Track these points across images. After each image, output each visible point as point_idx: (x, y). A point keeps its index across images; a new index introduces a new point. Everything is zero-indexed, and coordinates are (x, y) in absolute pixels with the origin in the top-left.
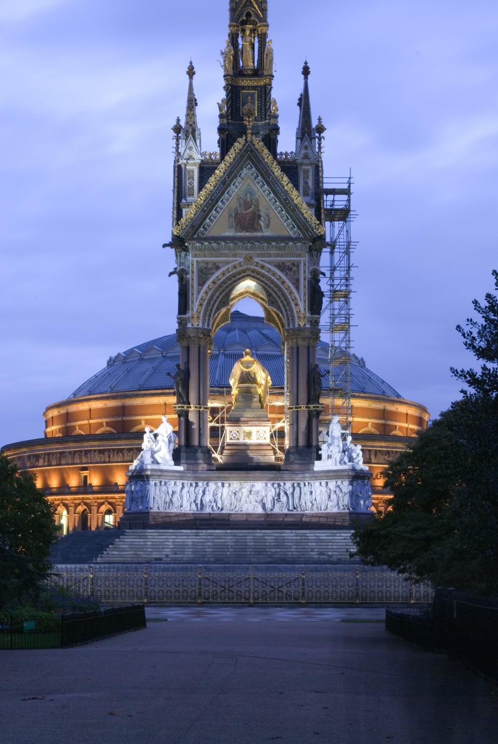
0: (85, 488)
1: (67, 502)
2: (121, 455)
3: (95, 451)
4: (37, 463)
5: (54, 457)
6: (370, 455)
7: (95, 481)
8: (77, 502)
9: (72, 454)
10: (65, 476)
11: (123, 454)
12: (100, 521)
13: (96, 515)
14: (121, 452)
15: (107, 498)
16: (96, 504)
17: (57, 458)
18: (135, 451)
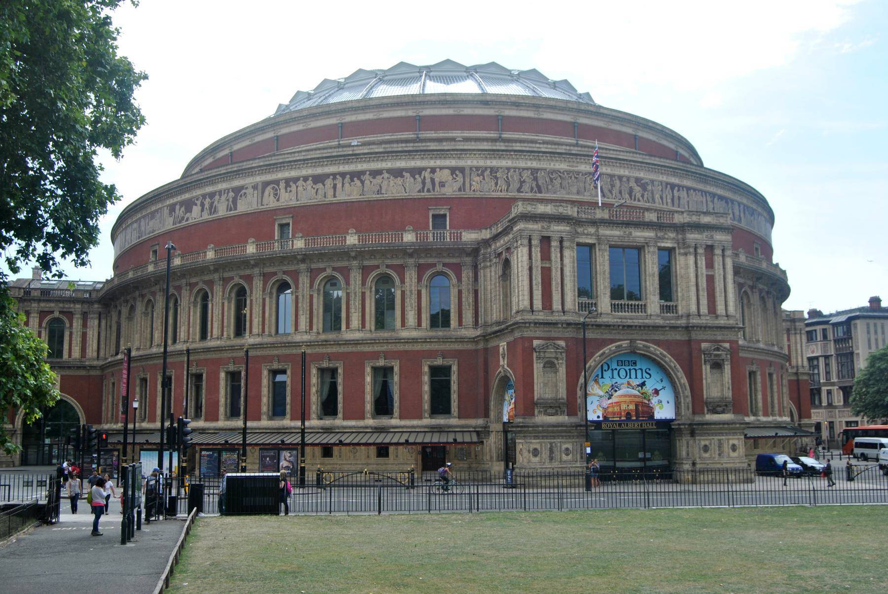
2: (357, 182)
3: (306, 179)
4: (188, 214)
5: (223, 198)
9: (260, 187)
11: (362, 182)
14: (359, 179)
17: (228, 200)
18: (386, 175)
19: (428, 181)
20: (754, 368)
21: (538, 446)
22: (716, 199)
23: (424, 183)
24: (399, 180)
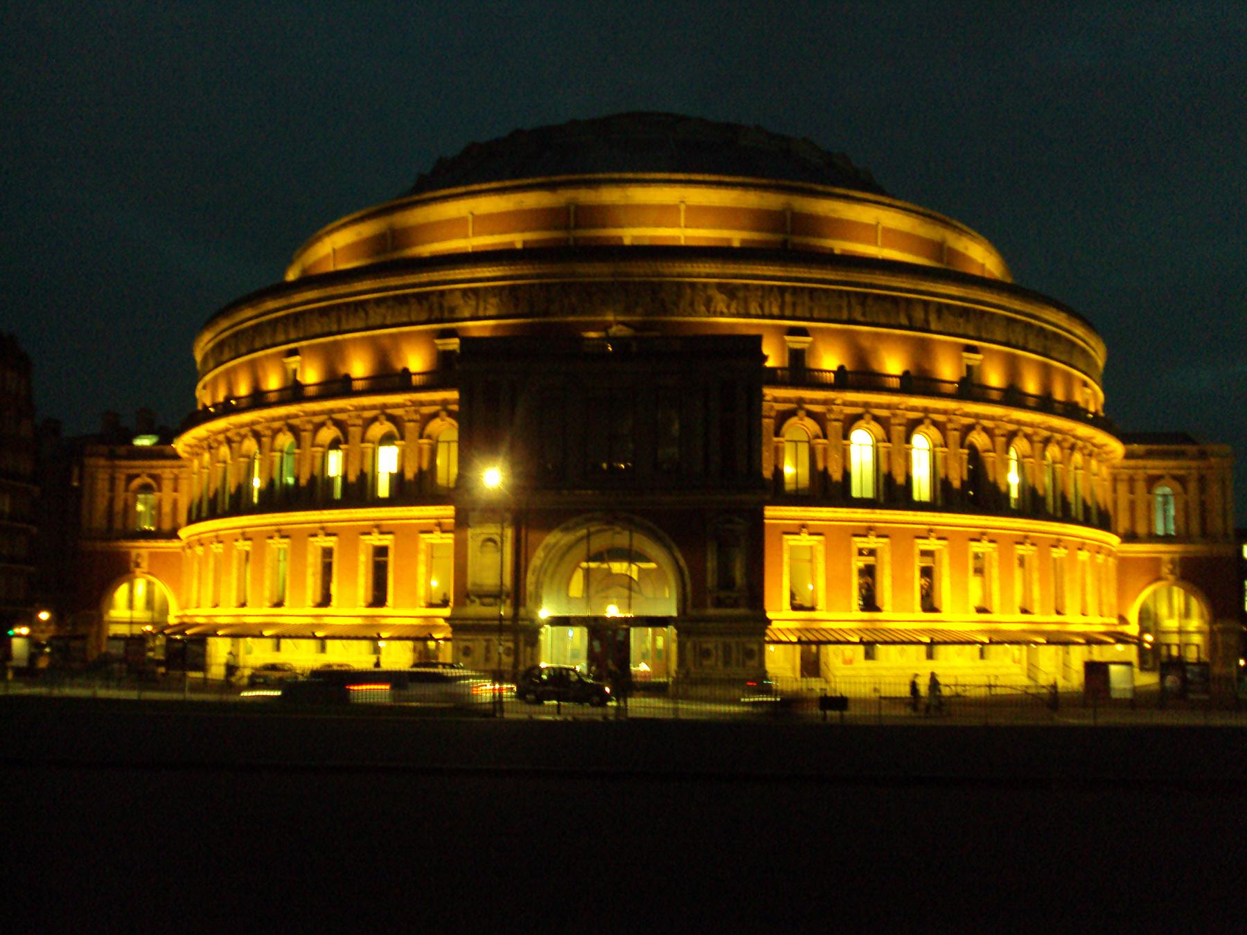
0: (294, 392)
1: (257, 428)
2: (362, 314)
3: (311, 311)
6: (926, 313)
7: (311, 376)
8: (276, 425)
10: (261, 374)
12: (318, 462)
13: (309, 451)
15: (331, 412)
16: (310, 427)
18: (390, 303)
19: (436, 306)
20: (932, 544)
21: (469, 644)
22: (870, 302)
23: (431, 309)
24: (405, 310)
